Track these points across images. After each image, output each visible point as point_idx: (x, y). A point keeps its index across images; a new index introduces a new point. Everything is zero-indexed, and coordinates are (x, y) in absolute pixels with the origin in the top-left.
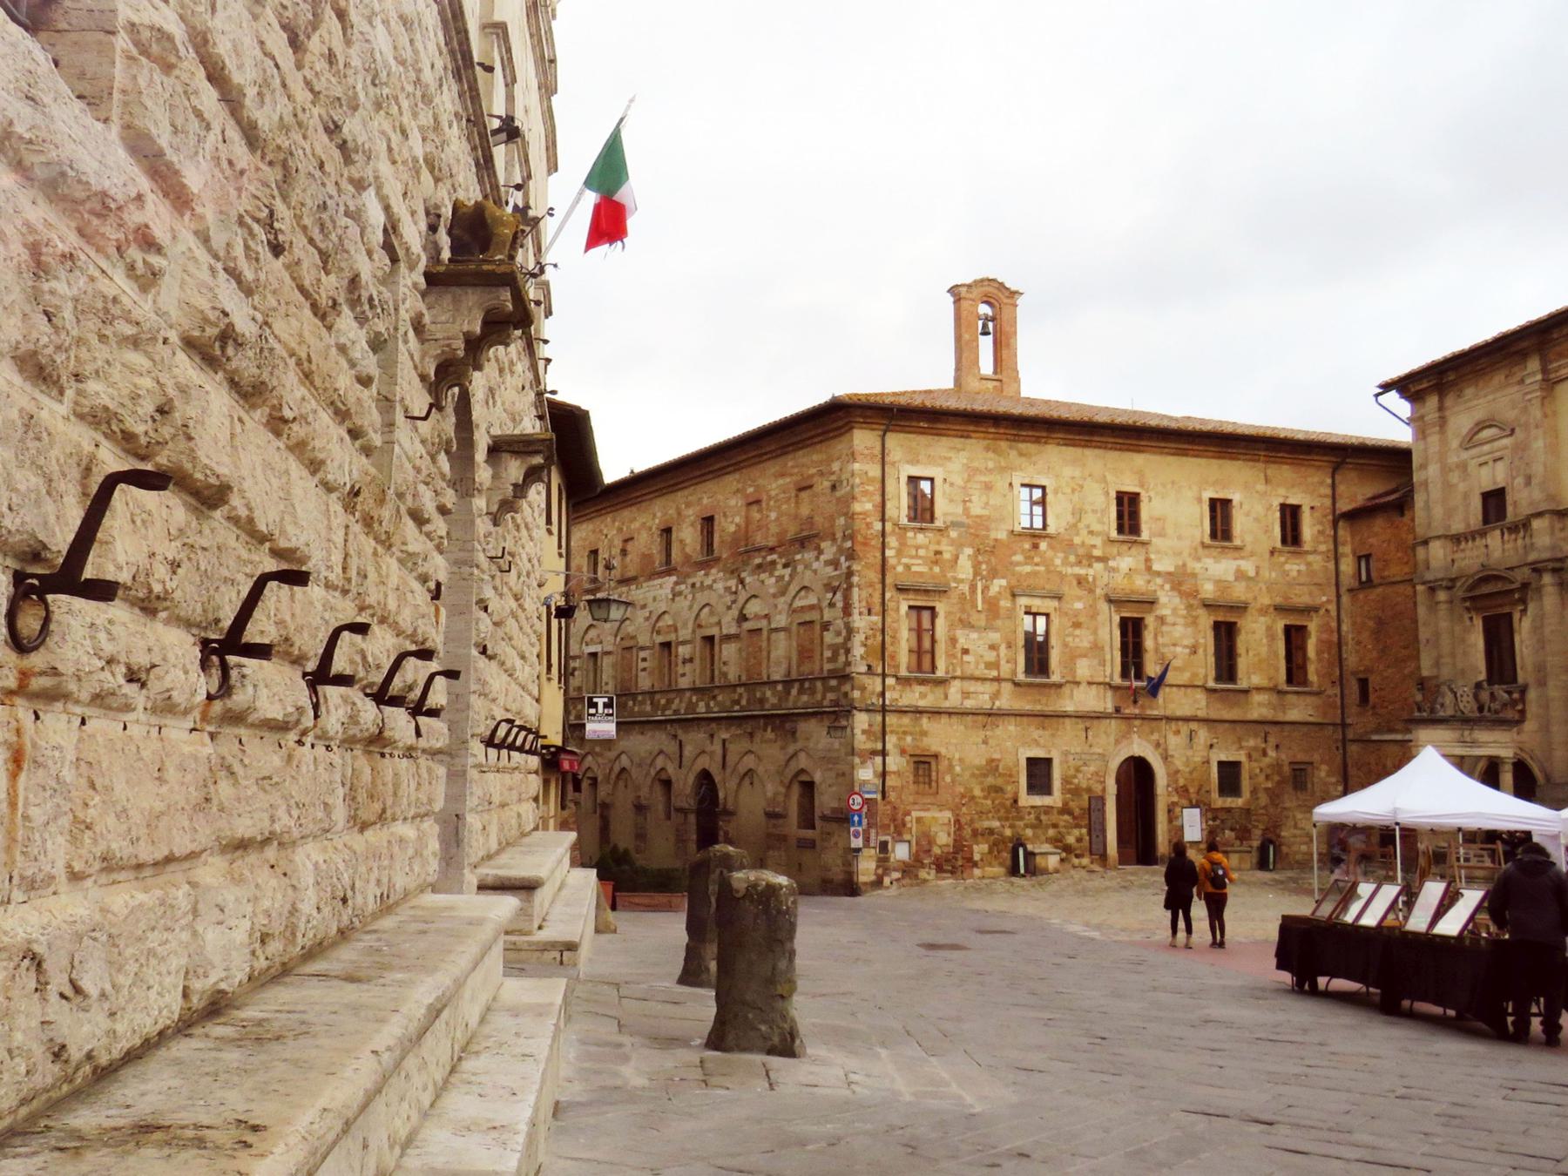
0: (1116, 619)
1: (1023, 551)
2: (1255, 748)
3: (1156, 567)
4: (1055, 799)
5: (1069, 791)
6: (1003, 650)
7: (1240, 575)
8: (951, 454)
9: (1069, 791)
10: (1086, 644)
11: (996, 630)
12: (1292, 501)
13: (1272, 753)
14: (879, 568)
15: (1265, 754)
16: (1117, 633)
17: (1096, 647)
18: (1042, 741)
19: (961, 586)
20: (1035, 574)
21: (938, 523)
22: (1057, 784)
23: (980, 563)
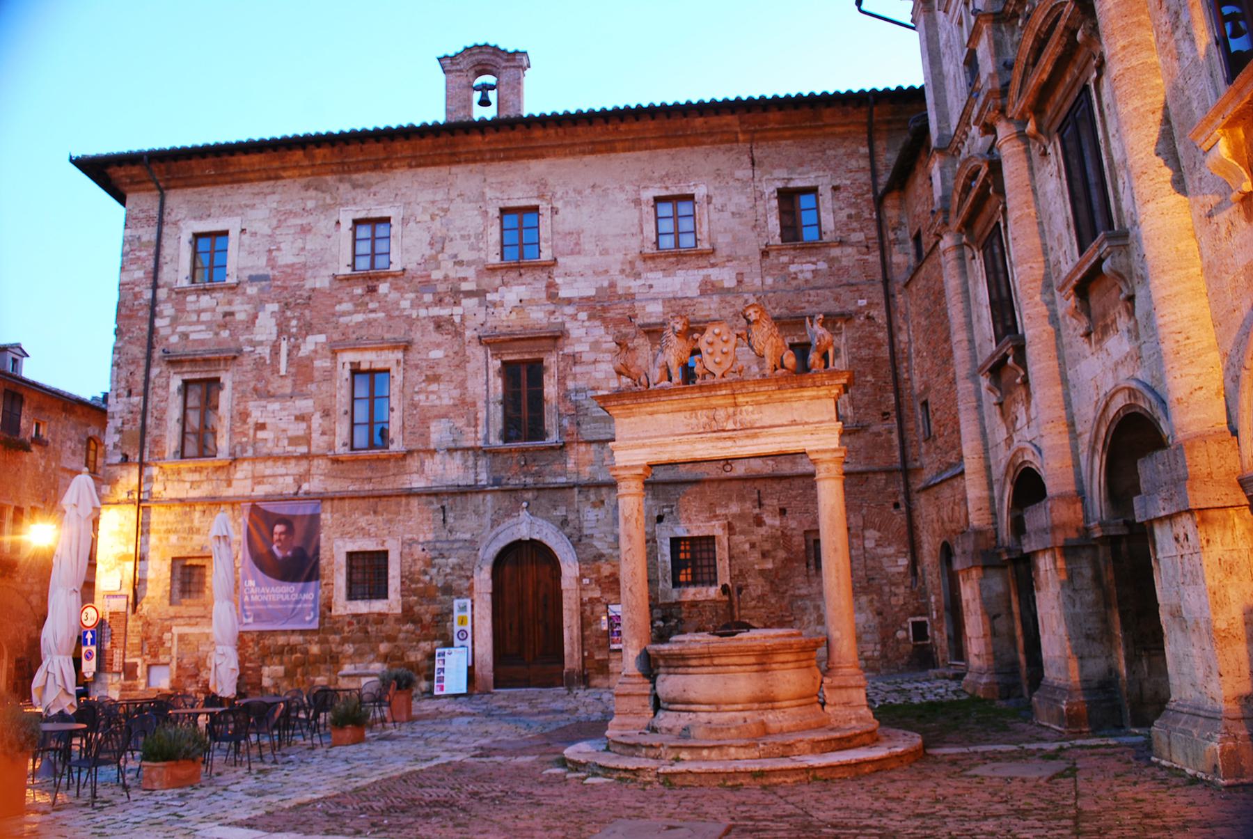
0: (497, 363)
1: (352, 298)
2: (741, 516)
3: (563, 294)
4: (392, 604)
5: (414, 592)
6: (317, 421)
7: (708, 288)
8: (257, 201)
9: (414, 592)
10: (447, 401)
11: (305, 396)
13: (772, 521)
14: (145, 342)
15: (759, 522)
16: (497, 385)
17: (464, 405)
18: (373, 529)
19: (259, 349)
20: (369, 323)
22: (394, 583)
23: (289, 319)
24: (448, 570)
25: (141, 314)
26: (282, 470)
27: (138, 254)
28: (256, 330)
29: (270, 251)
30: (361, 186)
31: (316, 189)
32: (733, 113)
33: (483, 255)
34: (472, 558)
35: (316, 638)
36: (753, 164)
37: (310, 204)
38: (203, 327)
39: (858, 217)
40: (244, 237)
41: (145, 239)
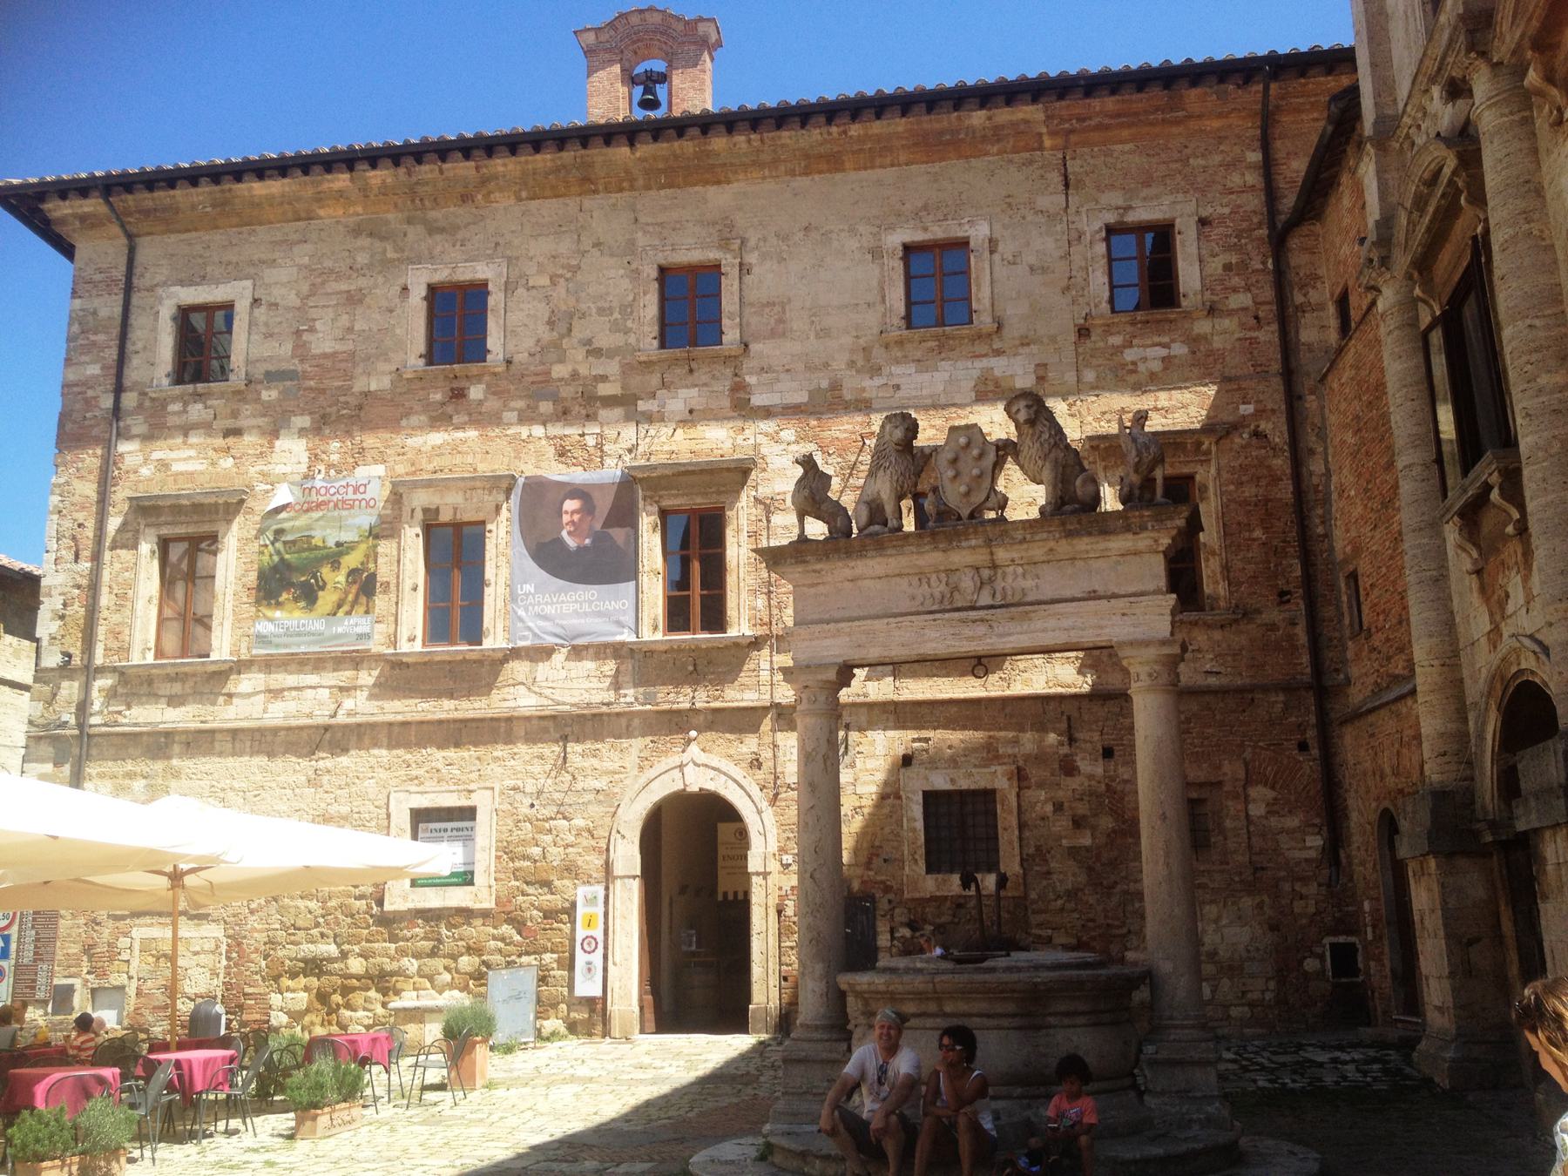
1: (427, 406)
2: (1040, 758)
3: (757, 400)
12: (1143, 213)
15: (1069, 768)
21: (237, 380)
24: (571, 839)
25: (95, 432)
26: (312, 679)
27: (92, 338)
28: (275, 457)
29: (298, 333)
30: (442, 230)
31: (371, 235)
32: (1035, 100)
33: (632, 339)
34: (608, 820)
35: (357, 949)
36: (1067, 185)
37: (362, 259)
38: (192, 453)
39: (1243, 266)
40: (257, 311)
41: (104, 313)
